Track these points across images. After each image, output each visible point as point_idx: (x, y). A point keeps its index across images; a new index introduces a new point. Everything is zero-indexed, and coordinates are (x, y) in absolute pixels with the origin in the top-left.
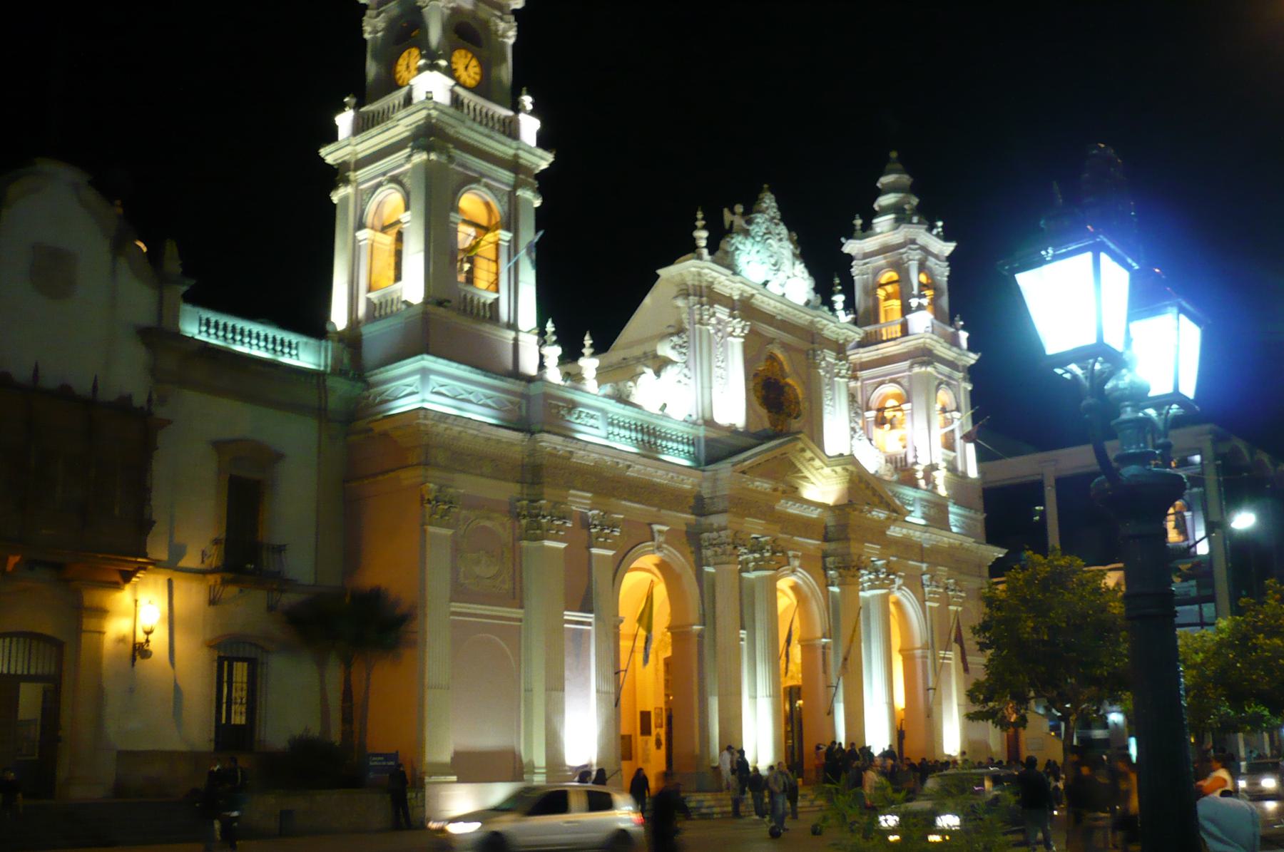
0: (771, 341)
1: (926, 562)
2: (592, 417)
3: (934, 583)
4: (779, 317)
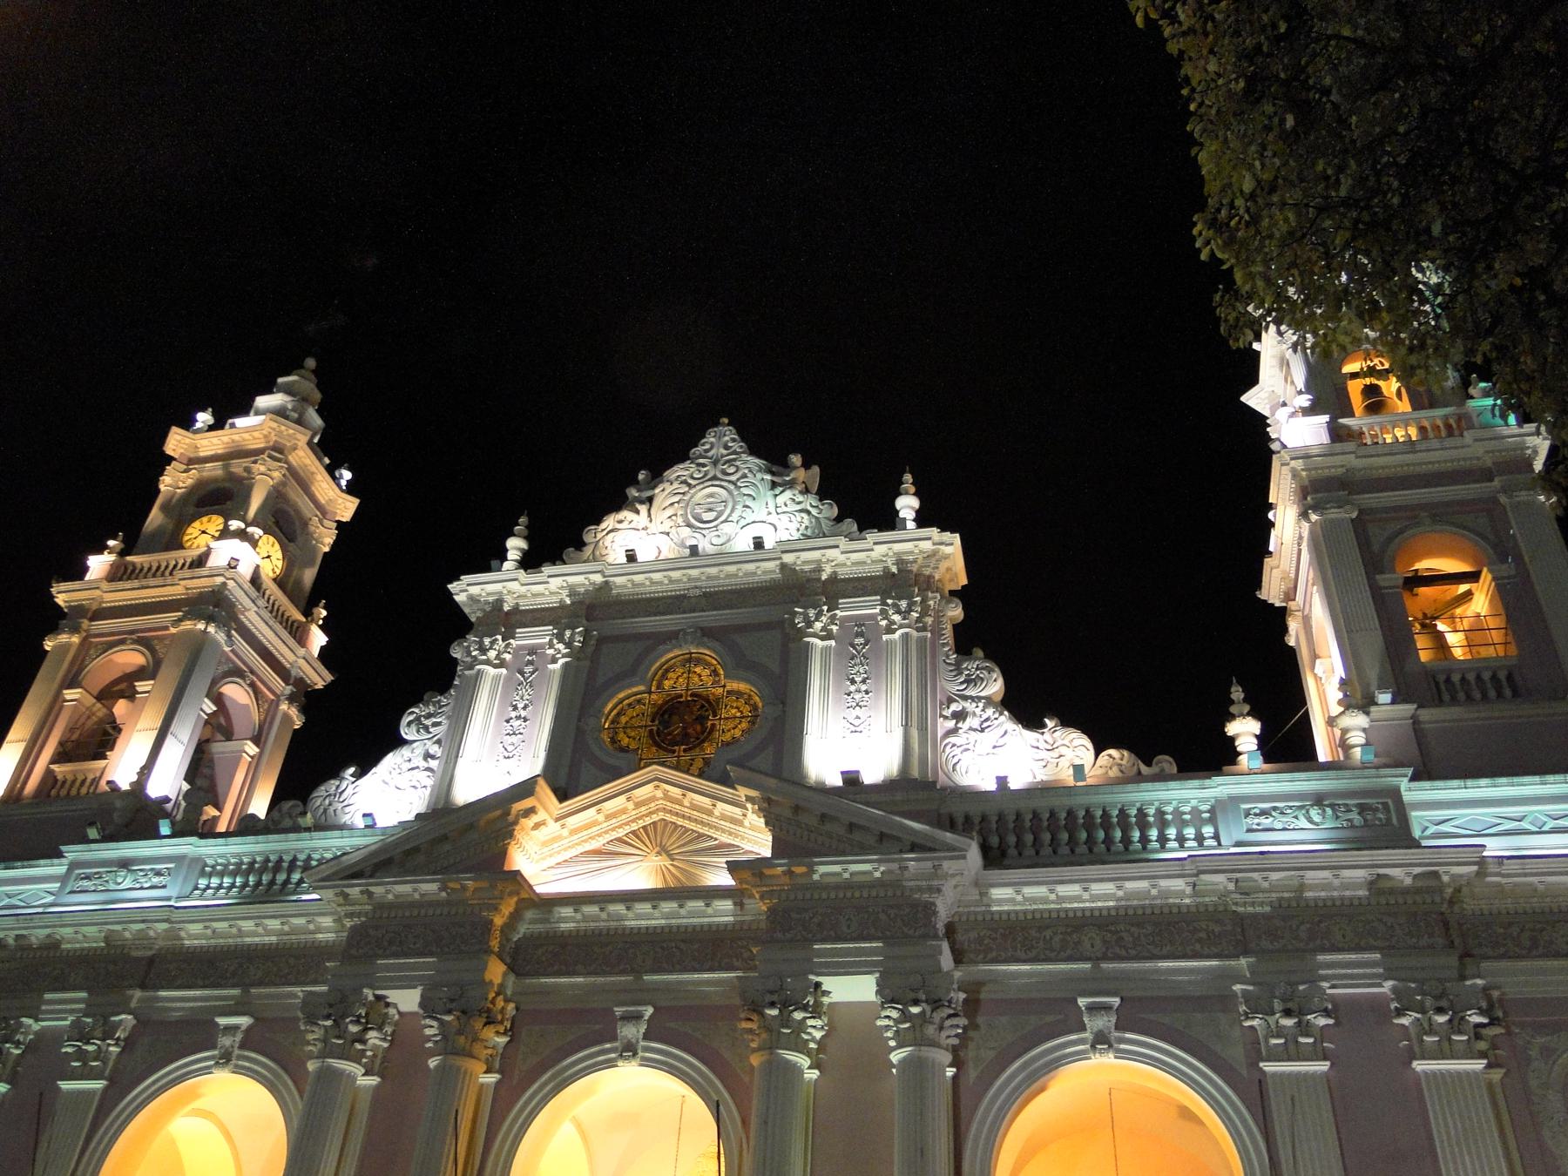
0: (672, 637)
1: (1246, 953)
2: (158, 873)
3: (1278, 1005)
4: (698, 592)
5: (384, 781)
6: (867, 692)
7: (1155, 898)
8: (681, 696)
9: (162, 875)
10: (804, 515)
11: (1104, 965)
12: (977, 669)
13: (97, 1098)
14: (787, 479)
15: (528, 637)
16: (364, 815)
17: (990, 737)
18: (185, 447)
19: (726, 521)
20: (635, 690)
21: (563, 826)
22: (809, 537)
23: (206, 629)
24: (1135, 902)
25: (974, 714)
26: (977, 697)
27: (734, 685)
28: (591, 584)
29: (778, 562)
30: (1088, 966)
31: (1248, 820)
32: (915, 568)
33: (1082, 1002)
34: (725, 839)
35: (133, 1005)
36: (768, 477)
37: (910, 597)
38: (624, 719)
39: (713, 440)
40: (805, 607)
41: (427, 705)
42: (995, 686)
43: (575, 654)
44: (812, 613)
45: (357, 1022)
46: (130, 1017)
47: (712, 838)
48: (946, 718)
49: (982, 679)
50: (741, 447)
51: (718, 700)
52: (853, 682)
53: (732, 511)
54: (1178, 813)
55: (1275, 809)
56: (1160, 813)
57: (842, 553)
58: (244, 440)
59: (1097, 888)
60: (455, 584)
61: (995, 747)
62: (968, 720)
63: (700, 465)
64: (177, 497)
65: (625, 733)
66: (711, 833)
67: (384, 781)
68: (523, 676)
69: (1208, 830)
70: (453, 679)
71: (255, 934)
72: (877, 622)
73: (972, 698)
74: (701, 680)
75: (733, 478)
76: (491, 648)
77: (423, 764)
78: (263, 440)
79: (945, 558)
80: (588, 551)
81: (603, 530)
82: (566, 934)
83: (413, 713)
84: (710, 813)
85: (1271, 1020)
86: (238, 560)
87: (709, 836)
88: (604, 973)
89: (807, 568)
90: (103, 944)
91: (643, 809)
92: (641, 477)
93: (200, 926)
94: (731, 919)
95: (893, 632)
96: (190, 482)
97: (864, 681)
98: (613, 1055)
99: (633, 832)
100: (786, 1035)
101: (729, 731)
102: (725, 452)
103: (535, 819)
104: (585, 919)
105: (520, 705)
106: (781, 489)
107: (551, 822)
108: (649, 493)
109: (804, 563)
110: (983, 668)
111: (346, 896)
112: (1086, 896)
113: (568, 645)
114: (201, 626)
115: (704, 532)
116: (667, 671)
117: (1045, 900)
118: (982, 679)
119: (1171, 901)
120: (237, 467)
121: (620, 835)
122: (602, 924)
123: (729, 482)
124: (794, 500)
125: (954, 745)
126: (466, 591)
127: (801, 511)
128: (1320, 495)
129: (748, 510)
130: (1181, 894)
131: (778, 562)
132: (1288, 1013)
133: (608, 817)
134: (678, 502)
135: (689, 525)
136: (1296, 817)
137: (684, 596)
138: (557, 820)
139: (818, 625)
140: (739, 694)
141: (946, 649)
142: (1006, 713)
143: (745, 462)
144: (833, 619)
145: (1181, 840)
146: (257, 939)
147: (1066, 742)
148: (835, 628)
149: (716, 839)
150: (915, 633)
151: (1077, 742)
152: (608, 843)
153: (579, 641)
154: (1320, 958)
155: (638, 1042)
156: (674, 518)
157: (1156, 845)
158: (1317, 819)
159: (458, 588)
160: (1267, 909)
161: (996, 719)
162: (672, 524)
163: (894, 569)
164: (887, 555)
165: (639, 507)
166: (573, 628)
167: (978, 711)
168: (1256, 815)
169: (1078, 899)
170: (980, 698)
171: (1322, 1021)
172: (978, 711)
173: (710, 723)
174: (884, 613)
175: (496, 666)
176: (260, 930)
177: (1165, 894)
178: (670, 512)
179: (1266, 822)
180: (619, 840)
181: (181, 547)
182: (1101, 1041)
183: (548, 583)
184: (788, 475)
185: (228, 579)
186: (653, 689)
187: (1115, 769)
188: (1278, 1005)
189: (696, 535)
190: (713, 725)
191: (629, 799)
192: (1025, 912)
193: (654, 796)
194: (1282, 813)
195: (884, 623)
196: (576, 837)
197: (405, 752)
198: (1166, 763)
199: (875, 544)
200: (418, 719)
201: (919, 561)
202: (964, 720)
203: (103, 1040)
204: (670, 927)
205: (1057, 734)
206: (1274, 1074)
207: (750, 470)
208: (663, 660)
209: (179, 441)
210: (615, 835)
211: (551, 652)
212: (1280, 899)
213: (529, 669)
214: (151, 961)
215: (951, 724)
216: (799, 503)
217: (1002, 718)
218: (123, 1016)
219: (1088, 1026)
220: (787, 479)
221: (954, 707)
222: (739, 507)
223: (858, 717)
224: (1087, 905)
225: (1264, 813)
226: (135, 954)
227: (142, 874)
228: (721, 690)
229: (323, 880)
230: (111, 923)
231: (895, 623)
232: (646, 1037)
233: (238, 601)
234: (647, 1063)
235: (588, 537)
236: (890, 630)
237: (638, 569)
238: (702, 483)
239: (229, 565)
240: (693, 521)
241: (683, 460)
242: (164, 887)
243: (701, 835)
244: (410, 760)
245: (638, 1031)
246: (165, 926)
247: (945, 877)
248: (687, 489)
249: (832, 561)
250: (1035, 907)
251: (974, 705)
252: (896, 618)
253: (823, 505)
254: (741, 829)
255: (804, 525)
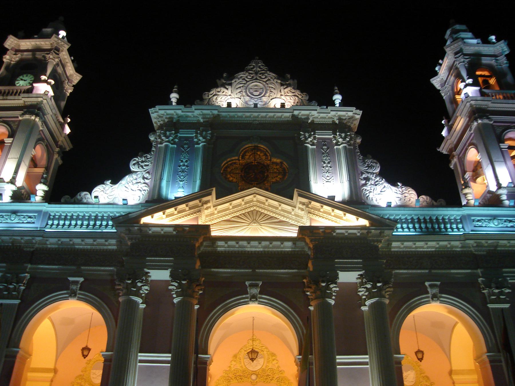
1: (480, 268)
2: (30, 217)
3: (493, 285)
4: (257, 122)
5: (125, 187)
6: (331, 167)
7: (449, 248)
8: (252, 163)
9: (32, 218)
10: (297, 98)
11: (433, 271)
12: (371, 162)
13: (17, 307)
14: (287, 83)
15: (183, 134)
16: (124, 200)
17: (379, 188)
18: (15, 44)
19: (264, 96)
20: (233, 158)
21: (216, 209)
22: (297, 105)
23: (35, 119)
24: (441, 249)
25: (372, 179)
26: (372, 173)
27: (275, 160)
28: (212, 114)
29: (291, 114)
30: (427, 271)
31: (474, 223)
32: (345, 122)
33: (427, 284)
34: (282, 219)
35: (28, 270)
36: (279, 81)
37: (345, 133)
38: (229, 170)
39: (254, 64)
40: (305, 132)
41: (141, 157)
42: (378, 170)
43: (208, 142)
44: (307, 135)
45: (141, 282)
46: (29, 275)
47: (277, 218)
48: (361, 179)
49: (374, 166)
50: (266, 69)
51: (268, 165)
52: (325, 163)
53: (266, 93)
54: (450, 219)
55: (482, 219)
56: (443, 219)
57: (318, 113)
58: (41, 45)
59: (430, 244)
60: (152, 109)
61: (381, 192)
62: (370, 181)
63: (250, 73)
64: (11, 65)
65: (230, 175)
66: (276, 216)
67: (125, 187)
68: (184, 149)
69: (460, 226)
70: (152, 148)
71: (81, 245)
72: (332, 141)
73: (371, 173)
74: (260, 157)
75: (265, 80)
76: (170, 136)
77: (142, 181)
78: (50, 46)
79: (356, 120)
80: (206, 102)
81: (211, 94)
82: (220, 252)
83: (135, 160)
84: (277, 208)
85: (491, 290)
86: (49, 92)
87: (275, 217)
88: (236, 268)
89: (303, 117)
90: (10, 244)
91: (248, 205)
92: (225, 75)
93: (56, 240)
94: (290, 249)
95: (339, 145)
96: (17, 59)
97: (329, 163)
98: (246, 300)
99: (243, 214)
100: (324, 294)
101: (275, 177)
102: (259, 70)
103: (209, 205)
104: (229, 246)
105: (184, 161)
106: (286, 86)
107: (212, 207)
108: (230, 82)
109: (302, 115)
110: (373, 162)
111: (130, 230)
112: (426, 246)
113: (204, 138)
114: (33, 118)
115: (255, 99)
116: (245, 152)
117: (411, 247)
118: (374, 166)
119: (454, 249)
120: (39, 55)
121: (237, 215)
122: (236, 249)
123: (263, 81)
124: (291, 91)
125: (366, 190)
126: (157, 112)
127: (295, 96)
128: (480, 114)
129: (272, 93)
130: (457, 247)
131: (291, 114)
132: (497, 288)
133: (234, 207)
134: (242, 87)
135: (248, 96)
136: (489, 223)
137: (251, 123)
138: (214, 207)
139: (310, 139)
140: (277, 164)
141: (359, 154)
142: (384, 179)
143: (269, 75)
144: (315, 138)
145: (457, 228)
146: (81, 247)
147: (407, 192)
148: (315, 141)
149: (278, 219)
150: (348, 147)
151: (410, 192)
152: (233, 217)
153: (209, 137)
154: (504, 270)
155: (257, 295)
156: (241, 92)
157: (444, 230)
158: (496, 224)
159: (154, 111)
160: (485, 253)
161: (380, 181)
162: (241, 95)
163: (337, 122)
164: (335, 116)
165: (227, 87)
166: (206, 131)
167: (373, 178)
168: (476, 221)
169: (422, 247)
170: (374, 173)
171: (508, 291)
172: (373, 178)
173: (266, 174)
174: (334, 137)
175: (172, 144)
176: (83, 243)
177: (452, 247)
178: (239, 90)
179: (480, 224)
180: (238, 217)
181: (15, 85)
182: (435, 297)
183: (193, 112)
184: (287, 82)
185: (44, 99)
186: (240, 159)
187: (425, 202)
188: (493, 285)
189: (251, 100)
190: (267, 175)
191: (243, 200)
192: (403, 251)
193: (253, 200)
194: (484, 221)
195: (334, 142)
196: (220, 214)
197: (134, 176)
198: (442, 201)
199: (331, 111)
200: (138, 162)
201: (347, 119)
202: (369, 181)
203: (17, 283)
204: (265, 251)
205: (404, 188)
206: (493, 309)
207: (271, 78)
208: (244, 147)
209: (13, 42)
210: (236, 214)
211: (195, 140)
212: (489, 250)
213: (186, 146)
214: (33, 252)
215: (364, 182)
216: (293, 93)
217: (383, 181)
218: (26, 274)
219: (430, 292)
220: (287, 83)
221: (364, 176)
222: (269, 91)
223: (328, 176)
224: (425, 250)
225: (478, 221)
226: (25, 249)
227: (22, 217)
228: (269, 162)
229: (120, 223)
230: (15, 236)
231: (339, 142)
232: (261, 293)
233: (46, 109)
234: (261, 303)
235: (205, 97)
236: (337, 144)
237: (231, 110)
238: (252, 80)
239: (45, 93)
240: (249, 94)
241: (243, 71)
242: (34, 223)
243: (272, 217)
244: (136, 179)
245: (257, 291)
246: (41, 238)
247: (384, 236)
248: (245, 82)
249: (313, 116)
250: (407, 250)
251: (372, 176)
252: (340, 140)
253: (303, 94)
254: (290, 215)
255: (296, 101)
